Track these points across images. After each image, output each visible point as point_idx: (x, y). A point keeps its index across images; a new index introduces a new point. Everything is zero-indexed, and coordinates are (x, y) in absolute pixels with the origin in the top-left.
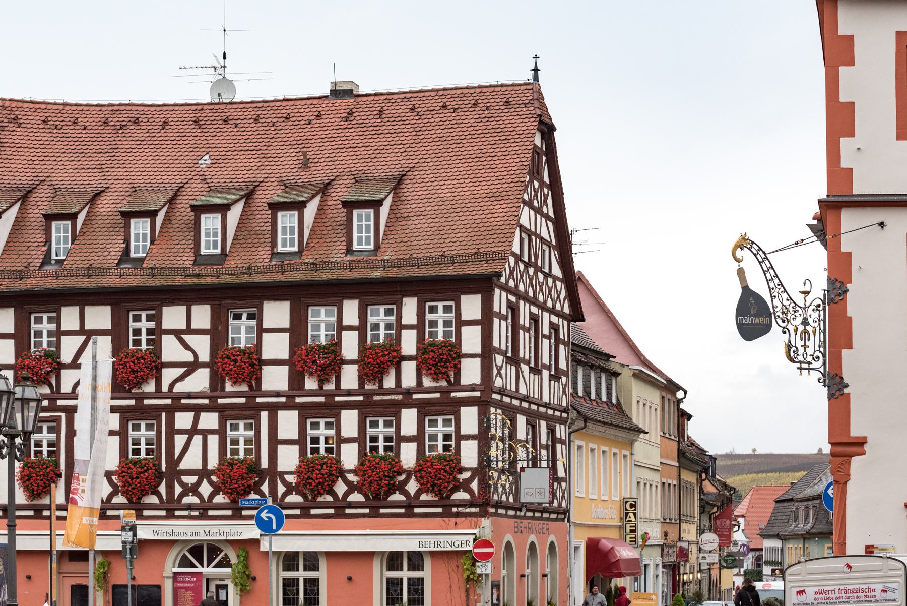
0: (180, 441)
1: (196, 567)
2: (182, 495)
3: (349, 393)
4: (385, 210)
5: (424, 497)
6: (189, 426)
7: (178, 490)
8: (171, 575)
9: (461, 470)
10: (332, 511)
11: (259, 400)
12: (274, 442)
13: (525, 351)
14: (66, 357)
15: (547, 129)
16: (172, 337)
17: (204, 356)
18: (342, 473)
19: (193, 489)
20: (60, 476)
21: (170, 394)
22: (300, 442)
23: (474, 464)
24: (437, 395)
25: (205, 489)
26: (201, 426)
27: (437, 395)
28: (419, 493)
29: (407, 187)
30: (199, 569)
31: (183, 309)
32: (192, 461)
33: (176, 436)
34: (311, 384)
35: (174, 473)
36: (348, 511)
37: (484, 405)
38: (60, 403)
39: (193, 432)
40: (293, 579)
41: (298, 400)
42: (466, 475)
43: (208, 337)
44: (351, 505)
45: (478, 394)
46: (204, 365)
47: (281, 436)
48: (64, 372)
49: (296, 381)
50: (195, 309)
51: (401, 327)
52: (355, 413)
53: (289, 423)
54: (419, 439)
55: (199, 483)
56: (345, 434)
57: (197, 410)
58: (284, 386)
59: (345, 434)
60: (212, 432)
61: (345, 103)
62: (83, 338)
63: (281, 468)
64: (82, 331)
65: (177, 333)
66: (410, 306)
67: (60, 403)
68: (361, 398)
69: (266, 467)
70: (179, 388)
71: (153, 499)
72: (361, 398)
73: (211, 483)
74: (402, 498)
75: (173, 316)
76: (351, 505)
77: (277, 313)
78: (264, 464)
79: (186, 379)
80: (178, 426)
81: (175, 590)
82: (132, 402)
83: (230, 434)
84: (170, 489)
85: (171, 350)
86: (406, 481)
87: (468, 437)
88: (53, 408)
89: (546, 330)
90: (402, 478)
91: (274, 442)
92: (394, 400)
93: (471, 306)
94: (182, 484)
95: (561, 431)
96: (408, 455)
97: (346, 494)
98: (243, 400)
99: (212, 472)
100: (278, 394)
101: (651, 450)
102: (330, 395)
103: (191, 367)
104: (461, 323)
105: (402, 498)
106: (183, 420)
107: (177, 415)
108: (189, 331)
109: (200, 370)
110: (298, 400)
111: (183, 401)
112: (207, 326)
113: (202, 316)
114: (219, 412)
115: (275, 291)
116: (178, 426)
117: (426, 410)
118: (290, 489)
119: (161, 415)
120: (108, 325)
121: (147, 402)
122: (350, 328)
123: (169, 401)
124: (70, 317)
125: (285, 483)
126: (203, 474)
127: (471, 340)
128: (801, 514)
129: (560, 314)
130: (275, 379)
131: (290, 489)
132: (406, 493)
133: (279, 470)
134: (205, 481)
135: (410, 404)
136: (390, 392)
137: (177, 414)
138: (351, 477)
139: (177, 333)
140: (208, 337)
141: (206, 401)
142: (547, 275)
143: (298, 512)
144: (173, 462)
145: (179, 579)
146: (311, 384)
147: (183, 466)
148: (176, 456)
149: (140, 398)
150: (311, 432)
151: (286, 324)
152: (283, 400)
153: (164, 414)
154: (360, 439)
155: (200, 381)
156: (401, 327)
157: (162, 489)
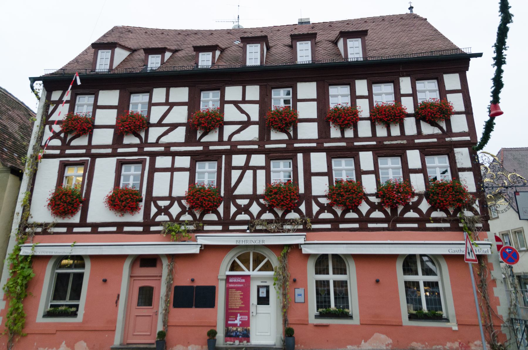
0: (235, 174)
1: (243, 270)
5: (434, 214)
6: (242, 164)
7: (233, 209)
8: (225, 277)
10: (357, 226)
11: (296, 145)
12: (309, 174)
14: (154, 119)
16: (232, 105)
17: (255, 116)
18: (365, 197)
19: (246, 209)
20: (141, 201)
24: (435, 140)
25: (255, 209)
26: (251, 164)
27: (435, 140)
28: (430, 211)
30: (246, 273)
31: (239, 89)
32: (245, 188)
34: (335, 133)
35: (231, 197)
36: (370, 225)
38: (146, 149)
40: (324, 281)
41: (326, 145)
43: (258, 105)
46: (254, 123)
47: (314, 170)
48: (151, 129)
49: (324, 133)
50: (248, 88)
52: (370, 154)
57: (249, 153)
58: (315, 135)
62: (167, 108)
63: (314, 193)
64: (167, 103)
65: (236, 103)
67: (146, 149)
68: (374, 143)
70: (235, 138)
71: (213, 217)
73: (259, 204)
74: (416, 215)
75: (233, 93)
77: (307, 90)
78: (302, 190)
79: (241, 132)
80: (234, 164)
81: (227, 290)
82: (200, 148)
84: (227, 209)
85: (231, 113)
86: (419, 202)
87: (463, 170)
88: (141, 153)
90: (416, 199)
91: (309, 174)
92: (401, 144)
93: (452, 81)
94: (236, 205)
96: (418, 183)
97: (369, 212)
98: (284, 146)
99: (262, 197)
103: (245, 125)
105: (416, 215)
106: (238, 160)
107: (234, 157)
108: (244, 101)
109: (252, 127)
110: (326, 145)
111: (239, 147)
112: (257, 98)
113: (253, 92)
114: (265, 154)
116: (234, 164)
117: (426, 151)
118: (323, 208)
119: (221, 157)
120: (186, 99)
121: (211, 148)
124: (159, 94)
125: (318, 203)
126: (254, 197)
130: (308, 131)
132: (419, 212)
134: (255, 203)
135: (414, 147)
136: (396, 138)
137: (233, 156)
138: (373, 199)
139: (236, 103)
140: (258, 105)
141: (256, 147)
143: (329, 226)
144: (230, 190)
145: (231, 281)
146: (335, 133)
147: (237, 192)
149: (207, 145)
151: (315, 96)
153: (224, 156)
155: (252, 133)
157: (221, 209)
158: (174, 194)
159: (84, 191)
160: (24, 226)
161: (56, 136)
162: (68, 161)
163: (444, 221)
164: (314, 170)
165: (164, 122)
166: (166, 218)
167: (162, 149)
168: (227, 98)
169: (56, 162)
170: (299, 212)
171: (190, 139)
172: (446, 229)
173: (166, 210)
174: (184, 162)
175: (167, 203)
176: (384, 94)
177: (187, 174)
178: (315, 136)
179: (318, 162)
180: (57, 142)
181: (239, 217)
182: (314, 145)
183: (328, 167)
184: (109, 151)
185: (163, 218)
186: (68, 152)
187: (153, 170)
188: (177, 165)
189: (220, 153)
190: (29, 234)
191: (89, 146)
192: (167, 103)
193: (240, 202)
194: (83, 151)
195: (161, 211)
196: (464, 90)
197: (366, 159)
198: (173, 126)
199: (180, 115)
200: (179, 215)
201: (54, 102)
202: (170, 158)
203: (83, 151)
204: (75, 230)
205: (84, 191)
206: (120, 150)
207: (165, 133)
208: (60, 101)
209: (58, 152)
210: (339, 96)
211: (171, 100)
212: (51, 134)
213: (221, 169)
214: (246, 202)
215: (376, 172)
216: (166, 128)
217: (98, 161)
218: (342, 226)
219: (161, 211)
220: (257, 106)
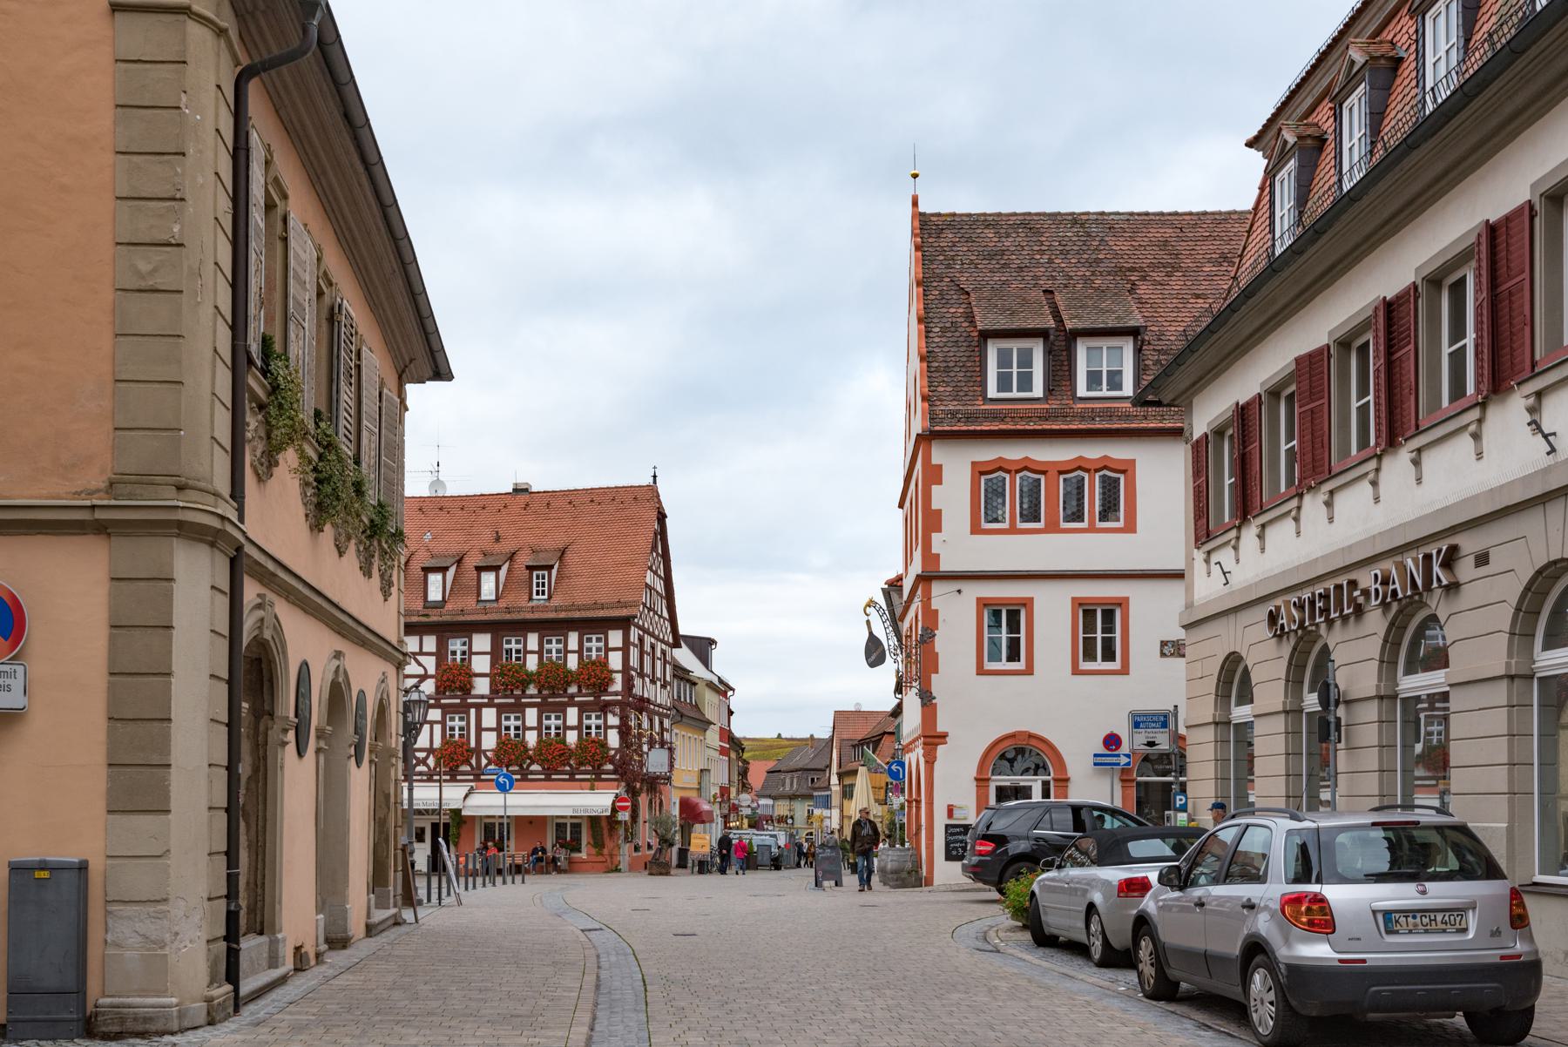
3: (531, 696)
4: (554, 572)
12: (479, 729)
13: (647, 669)
15: (662, 517)
17: (432, 671)
19: (424, 762)
22: (498, 729)
25: (431, 761)
29: (568, 556)
44: (532, 773)
47: (484, 725)
50: (426, 638)
51: (567, 652)
53: (489, 717)
54: (579, 728)
56: (528, 724)
59: (528, 724)
61: (523, 498)
66: (573, 640)
76: (532, 773)
77: (482, 642)
78: (473, 744)
83: (449, 724)
89: (658, 654)
93: (615, 638)
95: (667, 723)
100: (482, 697)
101: (713, 737)
102: (518, 698)
103: (423, 678)
104: (608, 649)
108: (421, 653)
113: (430, 643)
115: (481, 627)
122: (532, 652)
126: (430, 751)
127: (615, 661)
128: (788, 781)
129: (666, 643)
130: (482, 686)
131: (490, 762)
135: (573, 705)
142: (661, 616)
150: (505, 723)
151: (488, 649)
154: (539, 728)
155: (429, 687)
156: (567, 652)
181: (419, 769)
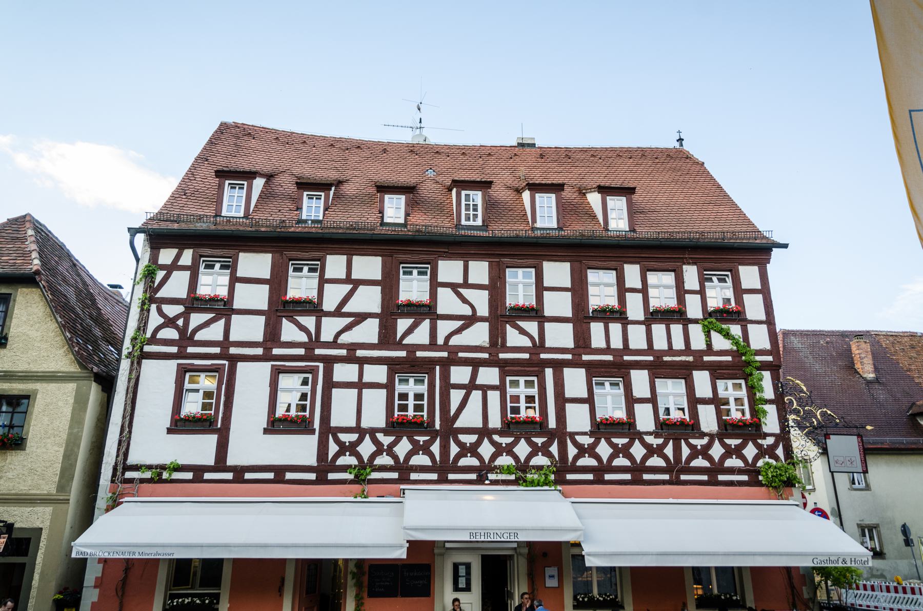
0: (456, 397)
2: (459, 456)
6: (466, 381)
7: (454, 449)
9: (765, 436)
10: (628, 477)
11: (543, 356)
12: (562, 400)
14: (329, 305)
16: (449, 290)
17: (483, 310)
18: (640, 436)
19: (473, 451)
21: (446, 346)
23: (776, 430)
24: (729, 358)
26: (479, 381)
27: (729, 358)
31: (460, 264)
32: (470, 418)
33: (452, 391)
35: (449, 431)
36: (646, 477)
37: (773, 368)
38: (318, 352)
39: (471, 386)
41: (585, 358)
42: (770, 441)
45: (770, 358)
46: (483, 319)
47: (568, 394)
55: (479, 443)
57: (476, 364)
60: (493, 388)
62: (350, 286)
63: (570, 429)
64: (348, 280)
65: (454, 287)
67: (318, 352)
68: (651, 358)
69: (555, 427)
70: (454, 341)
72: (651, 358)
75: (450, 270)
78: (552, 424)
80: (454, 379)
83: (511, 391)
84: (445, 449)
85: (447, 302)
90: (705, 441)
91: (562, 400)
93: (749, 275)
97: (645, 458)
98: (526, 356)
103: (470, 320)
106: (460, 375)
107: (453, 369)
108: (466, 285)
109: (479, 324)
110: (585, 358)
111: (461, 355)
112: (485, 281)
113: (480, 271)
114: (499, 367)
116: (454, 379)
121: (419, 354)
123: (445, 354)
126: (484, 432)
132: (710, 458)
133: (569, 430)
134: (486, 440)
135: (701, 365)
136: (680, 353)
138: (650, 439)
139: (454, 287)
141: (486, 356)
143: (590, 477)
144: (449, 420)
147: (458, 424)
148: (452, 413)
152: (569, 357)
153: (438, 367)
155: (479, 334)
158: (364, 424)
159: (221, 415)
160: (123, 465)
161: (170, 322)
162: (193, 365)
163: (740, 471)
164: (568, 394)
165: (345, 310)
166: (352, 461)
167: (343, 352)
168: (441, 279)
169: (172, 366)
170: (549, 455)
171: (387, 338)
172: (740, 484)
173: (352, 448)
174: (378, 373)
175: (354, 437)
176: (662, 289)
177: (384, 392)
178: (570, 344)
179: (575, 381)
180: (170, 333)
181: (463, 462)
182: (569, 357)
183: (588, 390)
184: (259, 351)
185: (347, 460)
186: (190, 350)
187: (330, 384)
188: (367, 379)
189: (433, 362)
190: (131, 481)
191: (226, 343)
192: (348, 280)
193: (463, 438)
194: (217, 350)
195: (344, 449)
196: (765, 291)
197: (640, 380)
198: (360, 318)
199: (369, 300)
200: (373, 457)
201: (162, 267)
202: (355, 367)
203: (217, 350)
204: (207, 476)
205: (221, 415)
206: (276, 351)
207: (348, 328)
208: (174, 266)
209: (174, 350)
210: (601, 288)
211: (354, 276)
212: (161, 320)
213: (435, 386)
214: (473, 438)
215: (653, 400)
216: (349, 320)
217: (240, 365)
218: (608, 477)
219: (344, 449)
220: (485, 294)
